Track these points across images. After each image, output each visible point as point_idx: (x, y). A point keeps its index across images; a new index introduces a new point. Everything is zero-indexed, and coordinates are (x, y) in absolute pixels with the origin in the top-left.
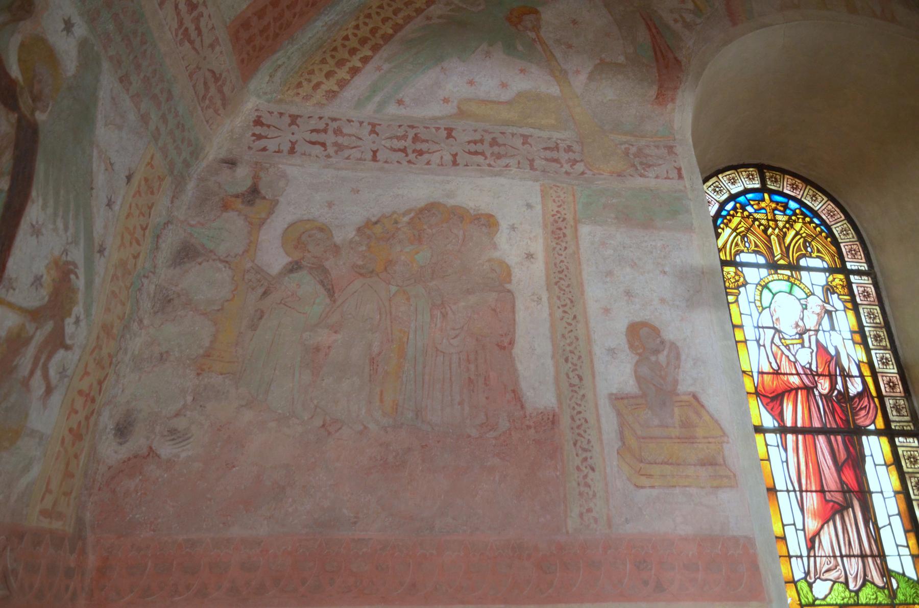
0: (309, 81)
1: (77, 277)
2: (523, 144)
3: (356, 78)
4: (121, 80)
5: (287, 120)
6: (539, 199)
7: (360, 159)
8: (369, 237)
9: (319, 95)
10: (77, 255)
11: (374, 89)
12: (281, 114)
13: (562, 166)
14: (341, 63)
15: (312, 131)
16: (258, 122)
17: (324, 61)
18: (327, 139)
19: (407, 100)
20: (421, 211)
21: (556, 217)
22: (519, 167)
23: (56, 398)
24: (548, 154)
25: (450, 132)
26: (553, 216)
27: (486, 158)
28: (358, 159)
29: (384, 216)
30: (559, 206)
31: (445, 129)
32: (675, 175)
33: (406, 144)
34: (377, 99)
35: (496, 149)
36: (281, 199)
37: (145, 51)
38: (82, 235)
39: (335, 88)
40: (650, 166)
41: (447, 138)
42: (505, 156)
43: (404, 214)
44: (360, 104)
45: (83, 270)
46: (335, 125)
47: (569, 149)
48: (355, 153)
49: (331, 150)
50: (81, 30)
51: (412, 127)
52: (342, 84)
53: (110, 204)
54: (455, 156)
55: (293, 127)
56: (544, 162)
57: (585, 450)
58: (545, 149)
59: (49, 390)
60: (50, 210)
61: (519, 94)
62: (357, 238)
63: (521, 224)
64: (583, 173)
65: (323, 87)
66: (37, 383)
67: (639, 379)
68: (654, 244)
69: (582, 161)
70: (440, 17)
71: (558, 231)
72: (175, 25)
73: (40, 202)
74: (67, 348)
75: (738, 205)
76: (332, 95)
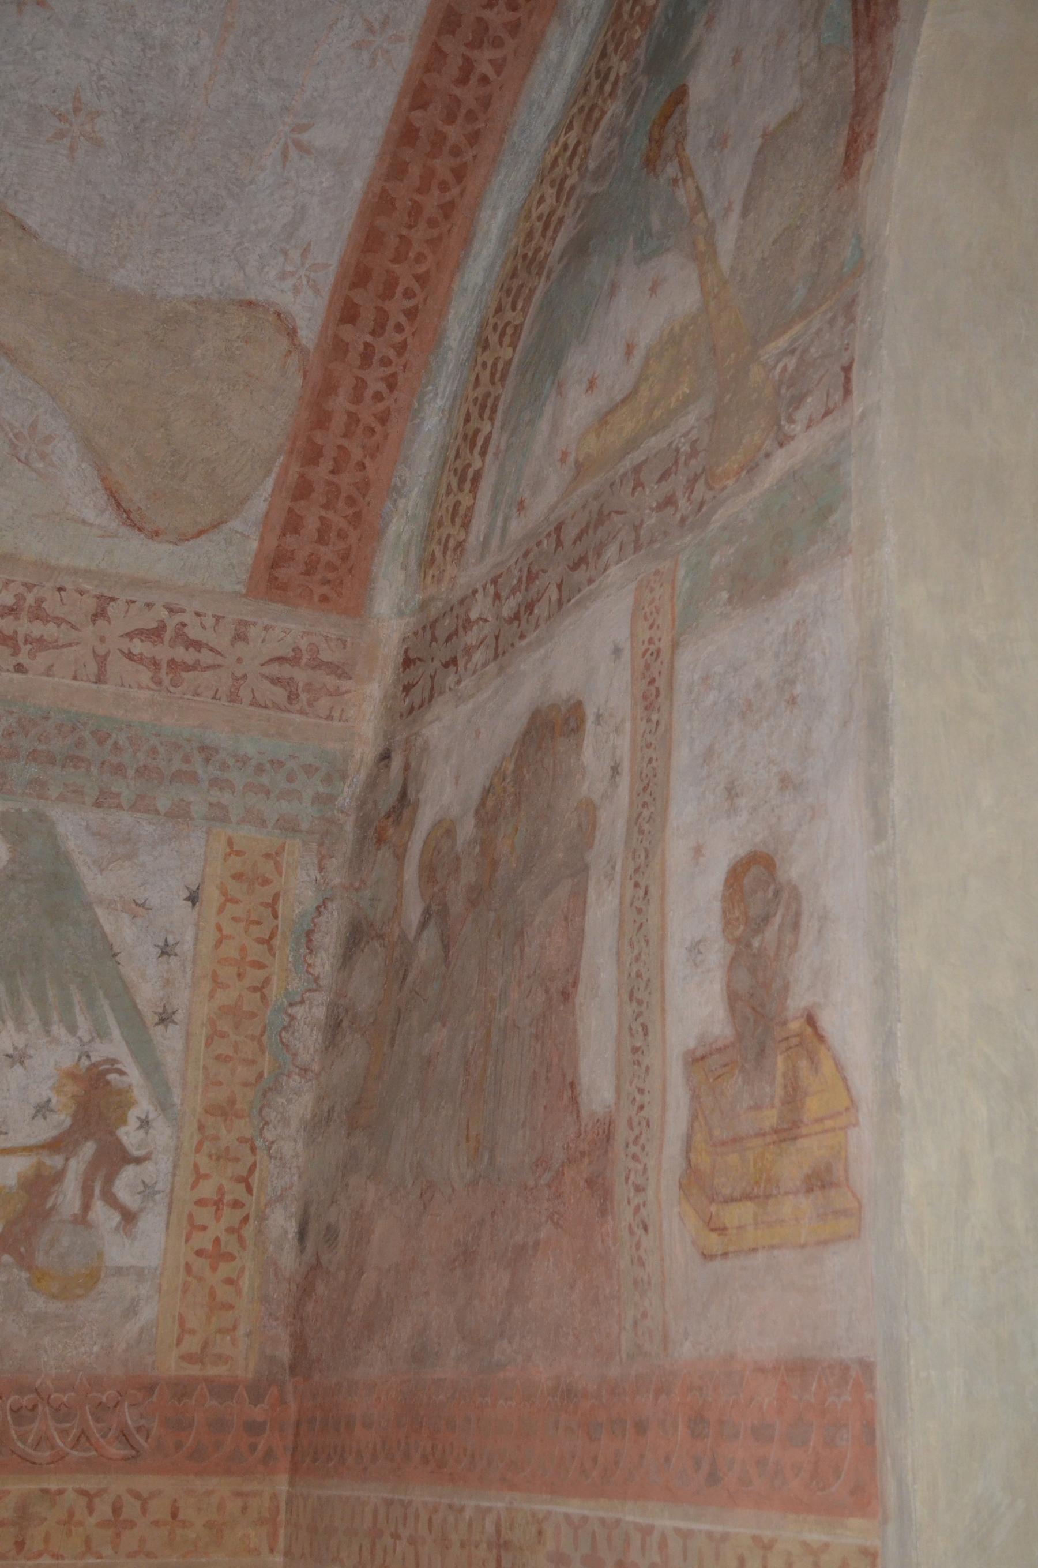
1: (122, 1073)
4: (98, 804)
10: (115, 1047)
23: (152, 1224)
37: (116, 743)
38: (112, 1021)
45: (130, 1060)
59: (129, 1217)
60: (34, 1024)
66: (101, 1213)
72: (145, 676)
74: (138, 1161)
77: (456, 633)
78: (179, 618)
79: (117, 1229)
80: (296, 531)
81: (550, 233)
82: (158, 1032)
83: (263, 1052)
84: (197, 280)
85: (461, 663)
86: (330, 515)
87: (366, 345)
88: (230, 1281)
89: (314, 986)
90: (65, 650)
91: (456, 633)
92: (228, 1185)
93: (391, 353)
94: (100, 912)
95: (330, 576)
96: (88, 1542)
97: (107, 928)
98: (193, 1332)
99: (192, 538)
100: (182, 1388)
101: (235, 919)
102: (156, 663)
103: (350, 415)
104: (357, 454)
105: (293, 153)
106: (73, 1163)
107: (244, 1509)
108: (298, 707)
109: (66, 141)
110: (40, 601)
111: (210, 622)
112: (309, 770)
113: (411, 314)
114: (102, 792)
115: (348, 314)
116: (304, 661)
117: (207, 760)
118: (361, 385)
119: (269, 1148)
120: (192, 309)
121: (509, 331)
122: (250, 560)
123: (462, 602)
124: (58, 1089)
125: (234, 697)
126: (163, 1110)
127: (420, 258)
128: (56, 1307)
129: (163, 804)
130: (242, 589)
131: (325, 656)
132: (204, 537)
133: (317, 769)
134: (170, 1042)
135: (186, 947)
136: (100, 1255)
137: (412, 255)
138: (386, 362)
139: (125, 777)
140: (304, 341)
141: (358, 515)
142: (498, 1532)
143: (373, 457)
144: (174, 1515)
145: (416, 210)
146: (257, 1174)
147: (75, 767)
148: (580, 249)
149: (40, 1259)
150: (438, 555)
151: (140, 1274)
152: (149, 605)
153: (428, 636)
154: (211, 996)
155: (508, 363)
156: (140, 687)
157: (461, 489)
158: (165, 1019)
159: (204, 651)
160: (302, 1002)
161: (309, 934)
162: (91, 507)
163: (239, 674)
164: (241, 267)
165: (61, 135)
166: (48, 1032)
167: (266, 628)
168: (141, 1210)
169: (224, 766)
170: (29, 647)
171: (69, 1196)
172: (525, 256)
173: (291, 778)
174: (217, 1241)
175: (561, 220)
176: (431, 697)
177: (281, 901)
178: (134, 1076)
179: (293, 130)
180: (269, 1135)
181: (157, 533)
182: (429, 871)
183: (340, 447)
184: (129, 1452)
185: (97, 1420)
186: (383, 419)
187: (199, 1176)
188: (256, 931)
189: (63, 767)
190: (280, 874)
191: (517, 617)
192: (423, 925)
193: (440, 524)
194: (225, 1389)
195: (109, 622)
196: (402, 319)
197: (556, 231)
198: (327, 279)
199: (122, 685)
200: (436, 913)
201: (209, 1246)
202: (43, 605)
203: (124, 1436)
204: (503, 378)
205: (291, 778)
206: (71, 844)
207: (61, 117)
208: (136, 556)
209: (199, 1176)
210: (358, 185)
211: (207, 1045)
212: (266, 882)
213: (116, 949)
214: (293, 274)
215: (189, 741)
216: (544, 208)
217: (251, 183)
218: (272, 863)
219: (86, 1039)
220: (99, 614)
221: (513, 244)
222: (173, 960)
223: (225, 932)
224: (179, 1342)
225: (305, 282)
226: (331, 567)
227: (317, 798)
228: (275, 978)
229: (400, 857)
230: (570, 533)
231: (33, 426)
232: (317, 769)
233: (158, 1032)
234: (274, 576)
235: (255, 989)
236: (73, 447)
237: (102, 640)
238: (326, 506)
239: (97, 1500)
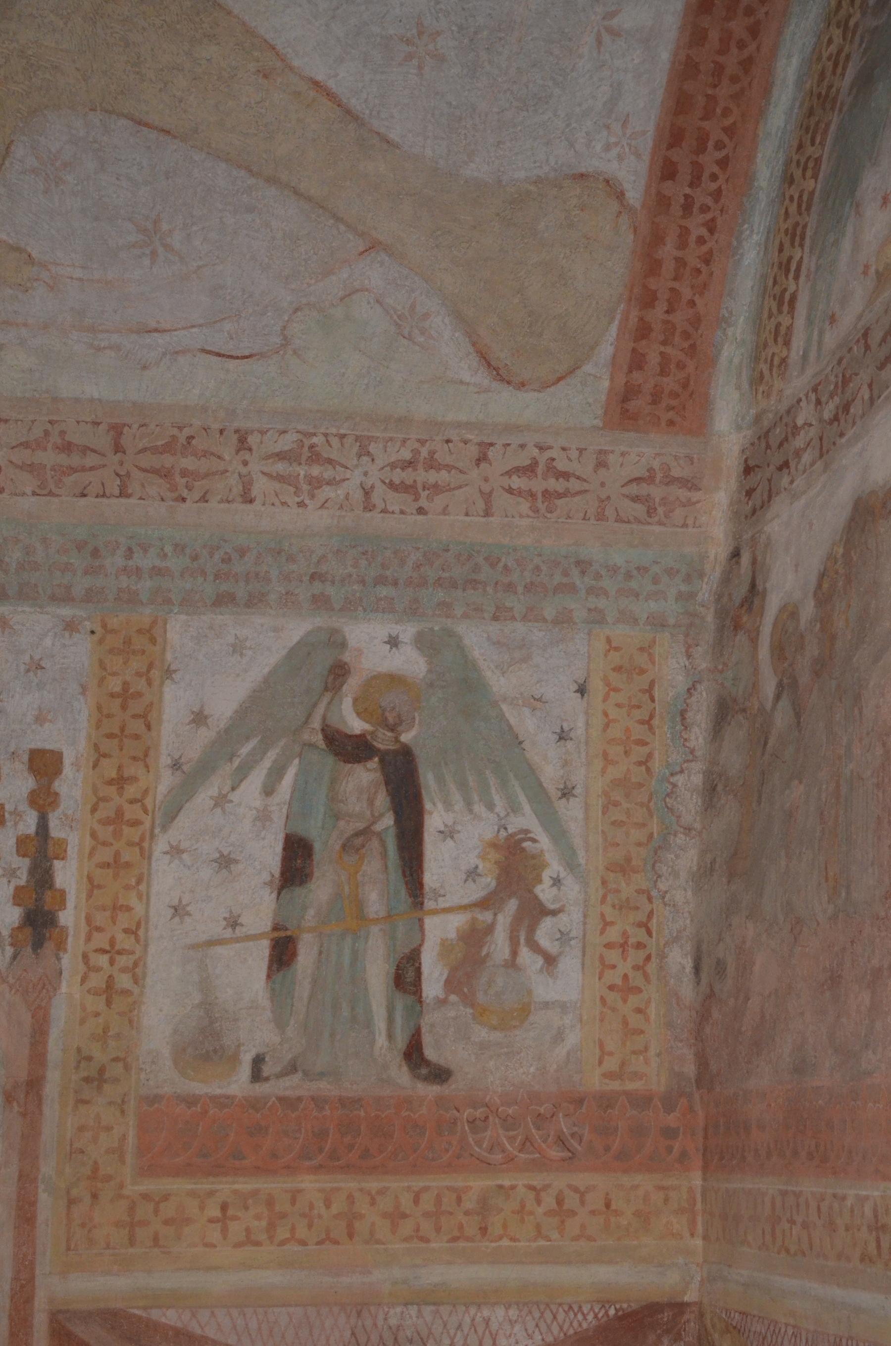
1: (534, 841)
4: (495, 618)
10: (526, 819)
23: (570, 964)
37: (506, 567)
38: (522, 799)
45: (540, 829)
50: (407, 631)
59: (550, 960)
60: (459, 805)
72: (525, 506)
73: (440, 806)
74: (554, 913)
77: (786, 439)
78: (548, 454)
79: (541, 970)
80: (640, 368)
81: (839, 71)
82: (561, 805)
83: (652, 817)
84: (535, 162)
85: (792, 464)
86: (668, 350)
87: (686, 196)
88: (639, 1011)
89: (691, 757)
90: (456, 492)
91: (786, 439)
92: (631, 930)
93: (709, 201)
94: (504, 707)
95: (674, 403)
96: (538, 1227)
97: (512, 721)
98: (611, 1054)
99: (554, 384)
100: (606, 1101)
101: (618, 705)
102: (532, 495)
103: (678, 260)
104: (687, 293)
105: (606, 38)
106: (500, 917)
107: (666, 1200)
108: (656, 519)
109: (415, 62)
110: (432, 453)
111: (574, 454)
112: (671, 572)
113: (723, 163)
114: (498, 608)
115: (667, 171)
116: (657, 480)
117: (583, 573)
118: (684, 232)
119: (664, 898)
120: (532, 188)
121: (811, 164)
122: (603, 398)
123: (788, 412)
124: (483, 857)
125: (601, 517)
126: (571, 870)
127: (726, 112)
128: (497, 1036)
129: (549, 612)
130: (598, 423)
131: (676, 472)
132: (562, 383)
133: (678, 571)
134: (572, 813)
135: (579, 732)
136: (530, 992)
137: (719, 111)
138: (705, 209)
139: (516, 593)
140: (631, 202)
141: (693, 347)
142: (876, 1216)
143: (701, 294)
144: (608, 1205)
145: (719, 69)
146: (654, 921)
147: (474, 589)
148: (865, 82)
149: (481, 997)
150: (766, 372)
151: (563, 1007)
152: (523, 446)
153: (763, 445)
154: (604, 771)
155: (812, 193)
156: (521, 516)
157: (780, 311)
158: (566, 793)
159: (572, 480)
160: (682, 771)
161: (683, 713)
162: (467, 370)
163: (603, 497)
164: (572, 145)
165: (409, 57)
166: (471, 811)
167: (623, 454)
168: (560, 954)
169: (598, 576)
170: (427, 492)
171: (499, 945)
172: (820, 94)
173: (656, 581)
174: (626, 976)
175: (848, 57)
176: (770, 497)
177: (656, 686)
178: (544, 842)
179: (604, 18)
180: (662, 886)
181: (523, 385)
182: (779, 651)
183: (672, 290)
184: (567, 1154)
185: (538, 1129)
186: (707, 260)
187: (606, 924)
188: (637, 714)
189: (464, 590)
190: (653, 663)
191: (836, 418)
192: (778, 697)
193: (765, 345)
194: (642, 1101)
195: (491, 464)
196: (716, 169)
197: (844, 68)
198: (647, 144)
199: (506, 516)
200: (787, 685)
201: (619, 981)
202: (435, 456)
203: (561, 1141)
204: (808, 209)
205: (656, 581)
206: (476, 653)
207: (408, 42)
208: (508, 405)
209: (606, 924)
210: (665, 56)
211: (604, 813)
212: (642, 671)
213: (521, 738)
214: (616, 144)
215: (566, 557)
216: (833, 48)
217: (572, 70)
218: (646, 655)
219: (502, 815)
220: (482, 459)
221: (808, 86)
222: (570, 745)
223: (611, 717)
224: (600, 1063)
225: (627, 150)
226: (674, 395)
227: (680, 597)
228: (656, 755)
229: (754, 641)
230: (877, 336)
231: (413, 307)
232: (678, 571)
233: (561, 805)
234: (626, 409)
235: (640, 763)
236: (447, 320)
237: (486, 480)
238: (664, 343)
239: (543, 1194)
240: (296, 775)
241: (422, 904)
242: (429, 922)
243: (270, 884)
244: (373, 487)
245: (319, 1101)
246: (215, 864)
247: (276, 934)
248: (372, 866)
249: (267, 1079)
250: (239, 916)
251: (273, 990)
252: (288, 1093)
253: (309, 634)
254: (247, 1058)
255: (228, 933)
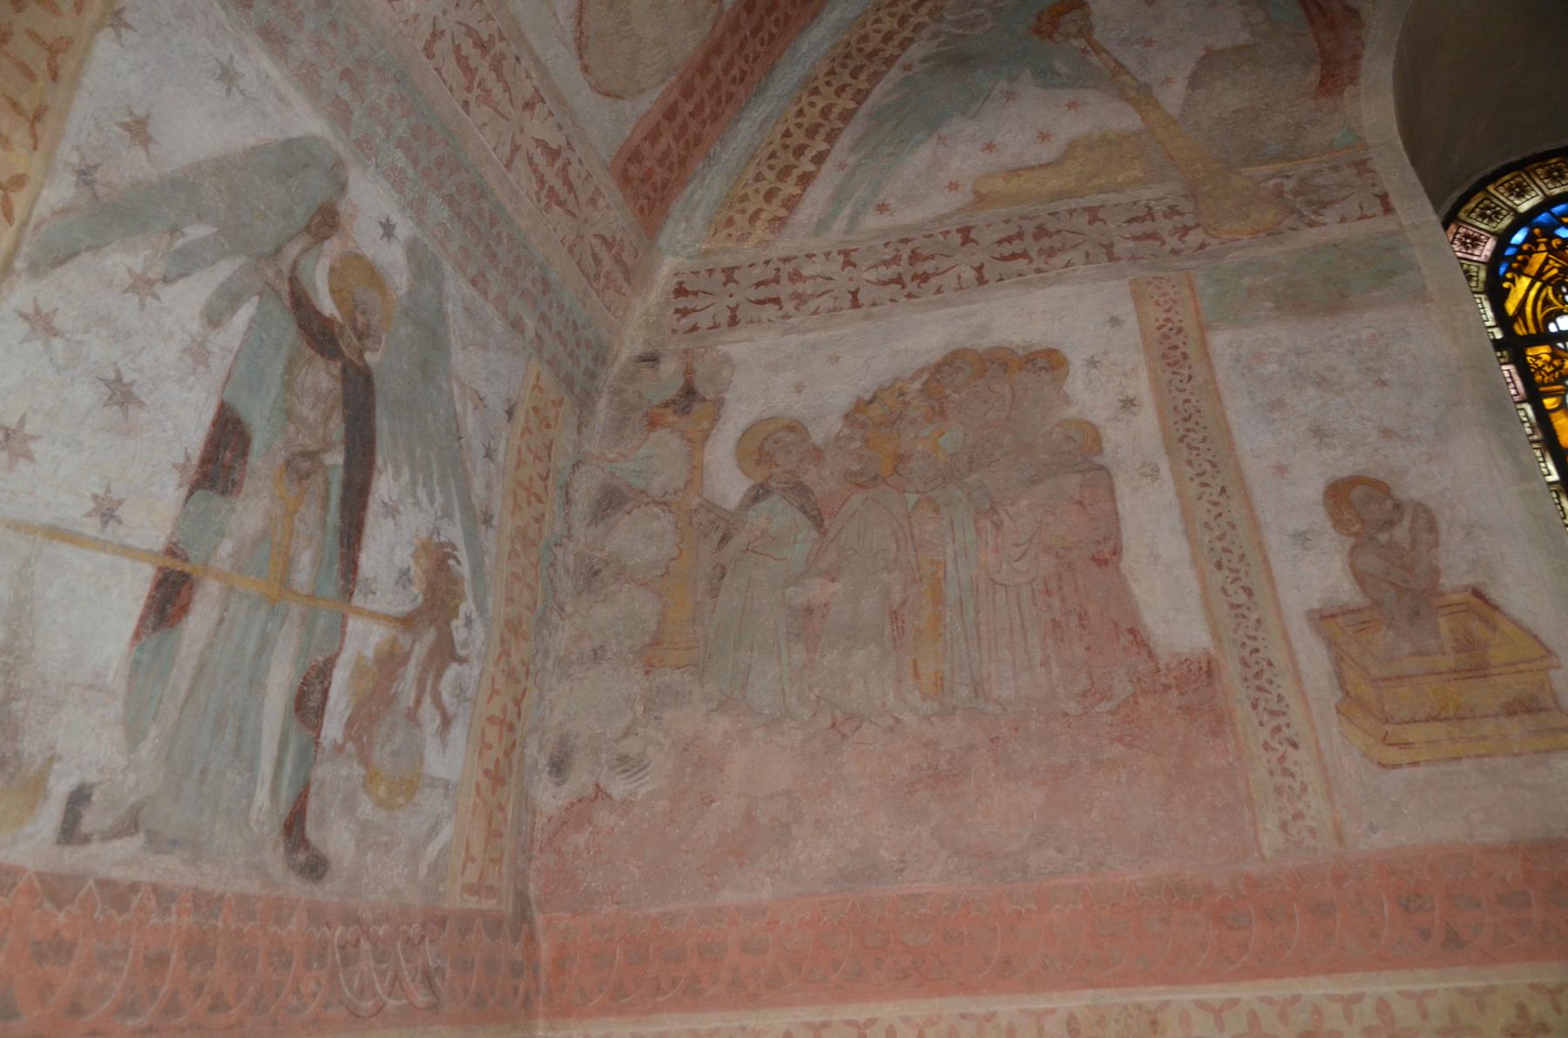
0: (744, 212)
1: (458, 562)
2: (1091, 222)
3: (810, 189)
4: (474, 282)
5: (721, 277)
6: (1130, 306)
7: (834, 309)
8: (863, 426)
9: (760, 231)
10: (454, 532)
11: (838, 198)
12: (710, 271)
13: (1164, 243)
14: (783, 174)
15: (758, 285)
16: (680, 291)
17: (759, 178)
18: (777, 293)
19: (891, 201)
20: (938, 368)
21: (1165, 330)
22: (1089, 263)
23: (458, 732)
24: (1136, 228)
25: (966, 234)
26: (1159, 328)
27: (1031, 260)
28: (830, 311)
29: (882, 389)
30: (1167, 311)
31: (959, 231)
32: (1378, 208)
33: (900, 270)
34: (847, 211)
35: (1046, 242)
36: (727, 396)
37: (499, 234)
38: (456, 505)
39: (783, 213)
40: (1325, 205)
41: (964, 244)
42: (1063, 249)
43: (913, 379)
44: (822, 226)
46: (789, 267)
47: (1173, 211)
48: (825, 302)
49: (789, 307)
50: (405, 229)
51: (905, 241)
52: (791, 204)
53: (489, 454)
54: (979, 269)
55: (731, 285)
56: (1131, 244)
57: (1273, 713)
58: (1130, 221)
59: (446, 721)
61: (1072, 146)
62: (847, 431)
63: (1106, 353)
64: (1202, 246)
65: (764, 215)
66: (428, 712)
67: (1360, 578)
68: (1354, 337)
69: (1197, 225)
70: (924, 60)
71: (1172, 352)
74: (462, 661)
75: (1537, 231)
76: (779, 223)
95: (652, 194)
124: (415, 556)
141: (685, 158)
229: (697, 442)
240: (253, 320)
241: (351, 594)
242: (354, 624)
243: (182, 469)
244: (442, 33)
245: (163, 896)
246: (104, 389)
247: (169, 562)
248: (310, 512)
249: (86, 839)
250: (120, 503)
251: (137, 662)
252: (117, 874)
253: (316, 139)
254: (61, 787)
255: (92, 528)
